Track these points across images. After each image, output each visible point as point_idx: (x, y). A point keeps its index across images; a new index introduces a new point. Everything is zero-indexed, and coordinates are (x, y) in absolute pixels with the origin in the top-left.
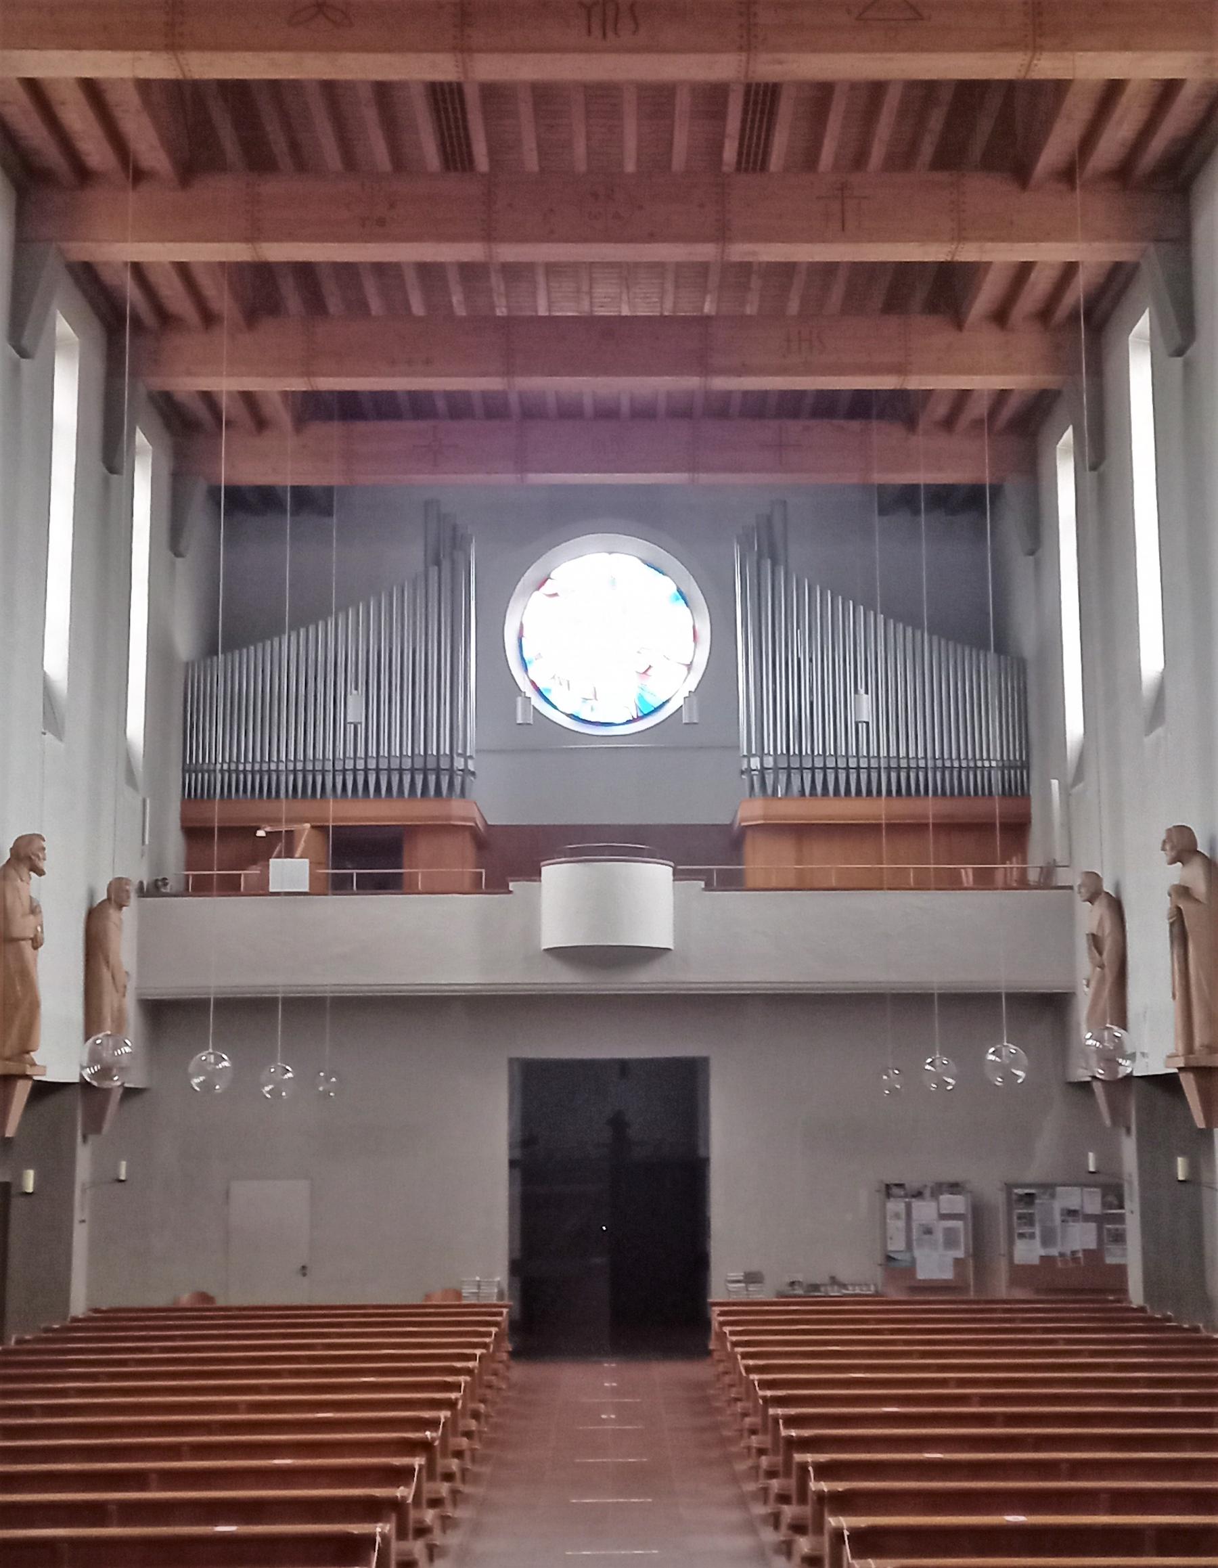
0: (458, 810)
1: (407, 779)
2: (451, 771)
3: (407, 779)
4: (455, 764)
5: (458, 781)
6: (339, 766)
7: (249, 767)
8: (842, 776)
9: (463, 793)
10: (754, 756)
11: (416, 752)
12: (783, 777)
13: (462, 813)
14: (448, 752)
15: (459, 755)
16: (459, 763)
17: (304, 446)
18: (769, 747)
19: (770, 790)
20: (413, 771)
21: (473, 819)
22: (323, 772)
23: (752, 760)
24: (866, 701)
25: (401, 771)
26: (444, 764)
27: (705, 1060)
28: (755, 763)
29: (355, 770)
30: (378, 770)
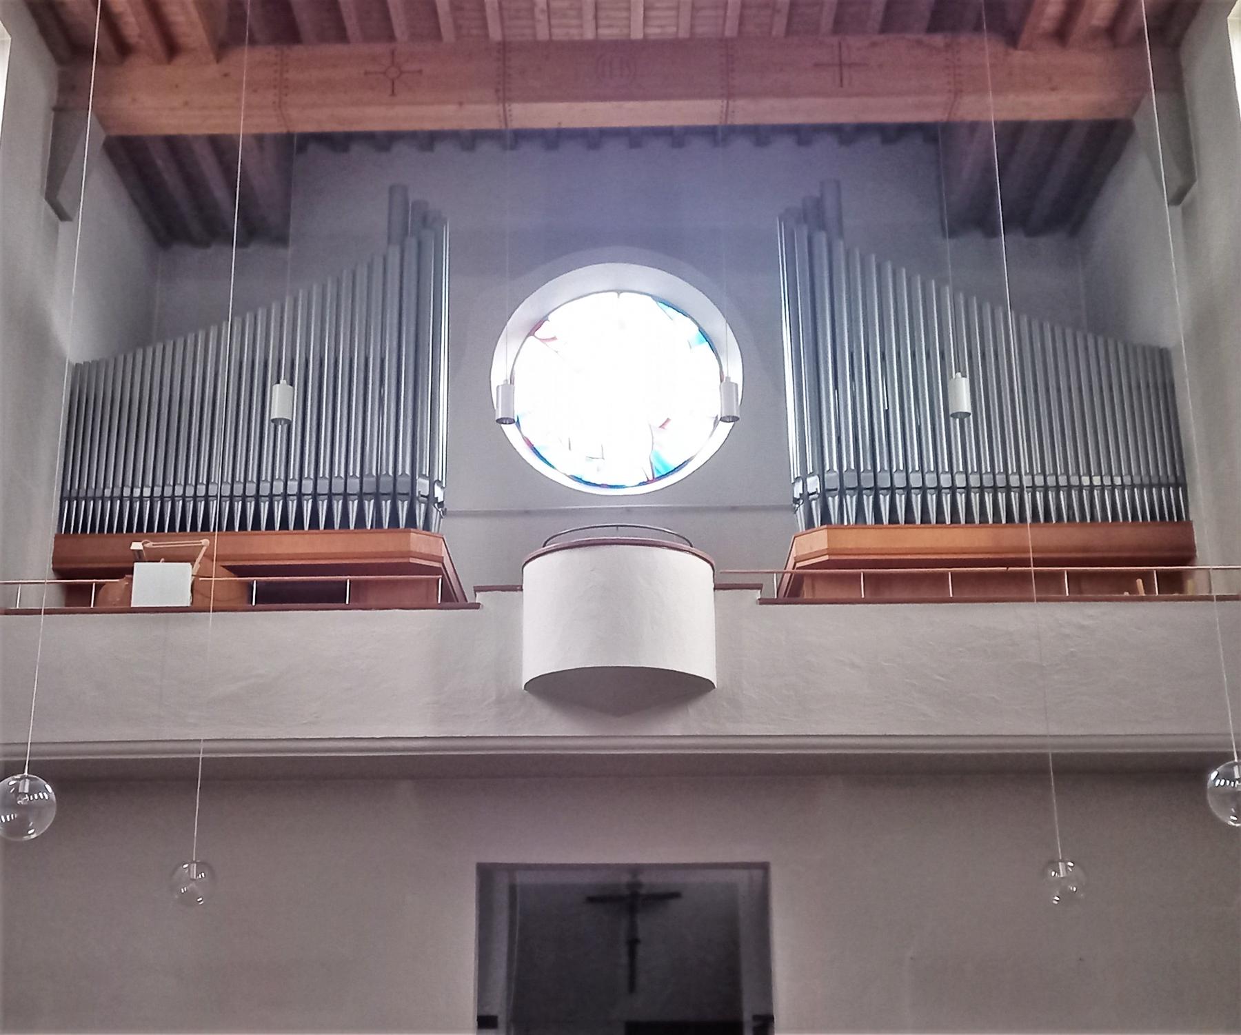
0: (417, 542)
1: (353, 507)
2: (412, 498)
3: (353, 507)
4: (418, 488)
5: (420, 510)
6: (265, 490)
7: (147, 492)
8: (932, 499)
9: (427, 527)
10: (812, 474)
11: (367, 472)
12: (851, 501)
13: (424, 550)
14: (408, 472)
15: (422, 476)
16: (423, 486)
17: (226, 75)
18: (831, 461)
19: (834, 518)
20: (361, 496)
21: (441, 560)
22: (244, 498)
23: (809, 480)
24: (962, 387)
25: (346, 496)
26: (403, 487)
27: (765, 867)
28: (813, 484)
29: (285, 496)
30: (315, 496)
